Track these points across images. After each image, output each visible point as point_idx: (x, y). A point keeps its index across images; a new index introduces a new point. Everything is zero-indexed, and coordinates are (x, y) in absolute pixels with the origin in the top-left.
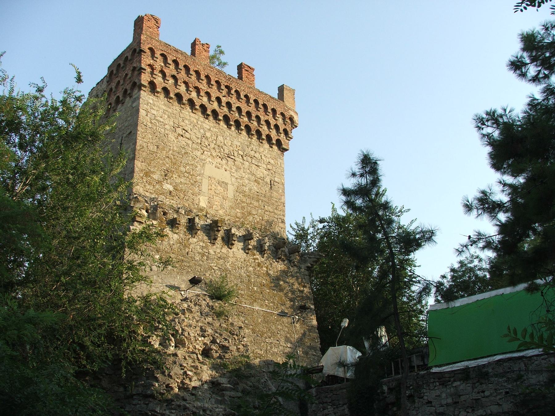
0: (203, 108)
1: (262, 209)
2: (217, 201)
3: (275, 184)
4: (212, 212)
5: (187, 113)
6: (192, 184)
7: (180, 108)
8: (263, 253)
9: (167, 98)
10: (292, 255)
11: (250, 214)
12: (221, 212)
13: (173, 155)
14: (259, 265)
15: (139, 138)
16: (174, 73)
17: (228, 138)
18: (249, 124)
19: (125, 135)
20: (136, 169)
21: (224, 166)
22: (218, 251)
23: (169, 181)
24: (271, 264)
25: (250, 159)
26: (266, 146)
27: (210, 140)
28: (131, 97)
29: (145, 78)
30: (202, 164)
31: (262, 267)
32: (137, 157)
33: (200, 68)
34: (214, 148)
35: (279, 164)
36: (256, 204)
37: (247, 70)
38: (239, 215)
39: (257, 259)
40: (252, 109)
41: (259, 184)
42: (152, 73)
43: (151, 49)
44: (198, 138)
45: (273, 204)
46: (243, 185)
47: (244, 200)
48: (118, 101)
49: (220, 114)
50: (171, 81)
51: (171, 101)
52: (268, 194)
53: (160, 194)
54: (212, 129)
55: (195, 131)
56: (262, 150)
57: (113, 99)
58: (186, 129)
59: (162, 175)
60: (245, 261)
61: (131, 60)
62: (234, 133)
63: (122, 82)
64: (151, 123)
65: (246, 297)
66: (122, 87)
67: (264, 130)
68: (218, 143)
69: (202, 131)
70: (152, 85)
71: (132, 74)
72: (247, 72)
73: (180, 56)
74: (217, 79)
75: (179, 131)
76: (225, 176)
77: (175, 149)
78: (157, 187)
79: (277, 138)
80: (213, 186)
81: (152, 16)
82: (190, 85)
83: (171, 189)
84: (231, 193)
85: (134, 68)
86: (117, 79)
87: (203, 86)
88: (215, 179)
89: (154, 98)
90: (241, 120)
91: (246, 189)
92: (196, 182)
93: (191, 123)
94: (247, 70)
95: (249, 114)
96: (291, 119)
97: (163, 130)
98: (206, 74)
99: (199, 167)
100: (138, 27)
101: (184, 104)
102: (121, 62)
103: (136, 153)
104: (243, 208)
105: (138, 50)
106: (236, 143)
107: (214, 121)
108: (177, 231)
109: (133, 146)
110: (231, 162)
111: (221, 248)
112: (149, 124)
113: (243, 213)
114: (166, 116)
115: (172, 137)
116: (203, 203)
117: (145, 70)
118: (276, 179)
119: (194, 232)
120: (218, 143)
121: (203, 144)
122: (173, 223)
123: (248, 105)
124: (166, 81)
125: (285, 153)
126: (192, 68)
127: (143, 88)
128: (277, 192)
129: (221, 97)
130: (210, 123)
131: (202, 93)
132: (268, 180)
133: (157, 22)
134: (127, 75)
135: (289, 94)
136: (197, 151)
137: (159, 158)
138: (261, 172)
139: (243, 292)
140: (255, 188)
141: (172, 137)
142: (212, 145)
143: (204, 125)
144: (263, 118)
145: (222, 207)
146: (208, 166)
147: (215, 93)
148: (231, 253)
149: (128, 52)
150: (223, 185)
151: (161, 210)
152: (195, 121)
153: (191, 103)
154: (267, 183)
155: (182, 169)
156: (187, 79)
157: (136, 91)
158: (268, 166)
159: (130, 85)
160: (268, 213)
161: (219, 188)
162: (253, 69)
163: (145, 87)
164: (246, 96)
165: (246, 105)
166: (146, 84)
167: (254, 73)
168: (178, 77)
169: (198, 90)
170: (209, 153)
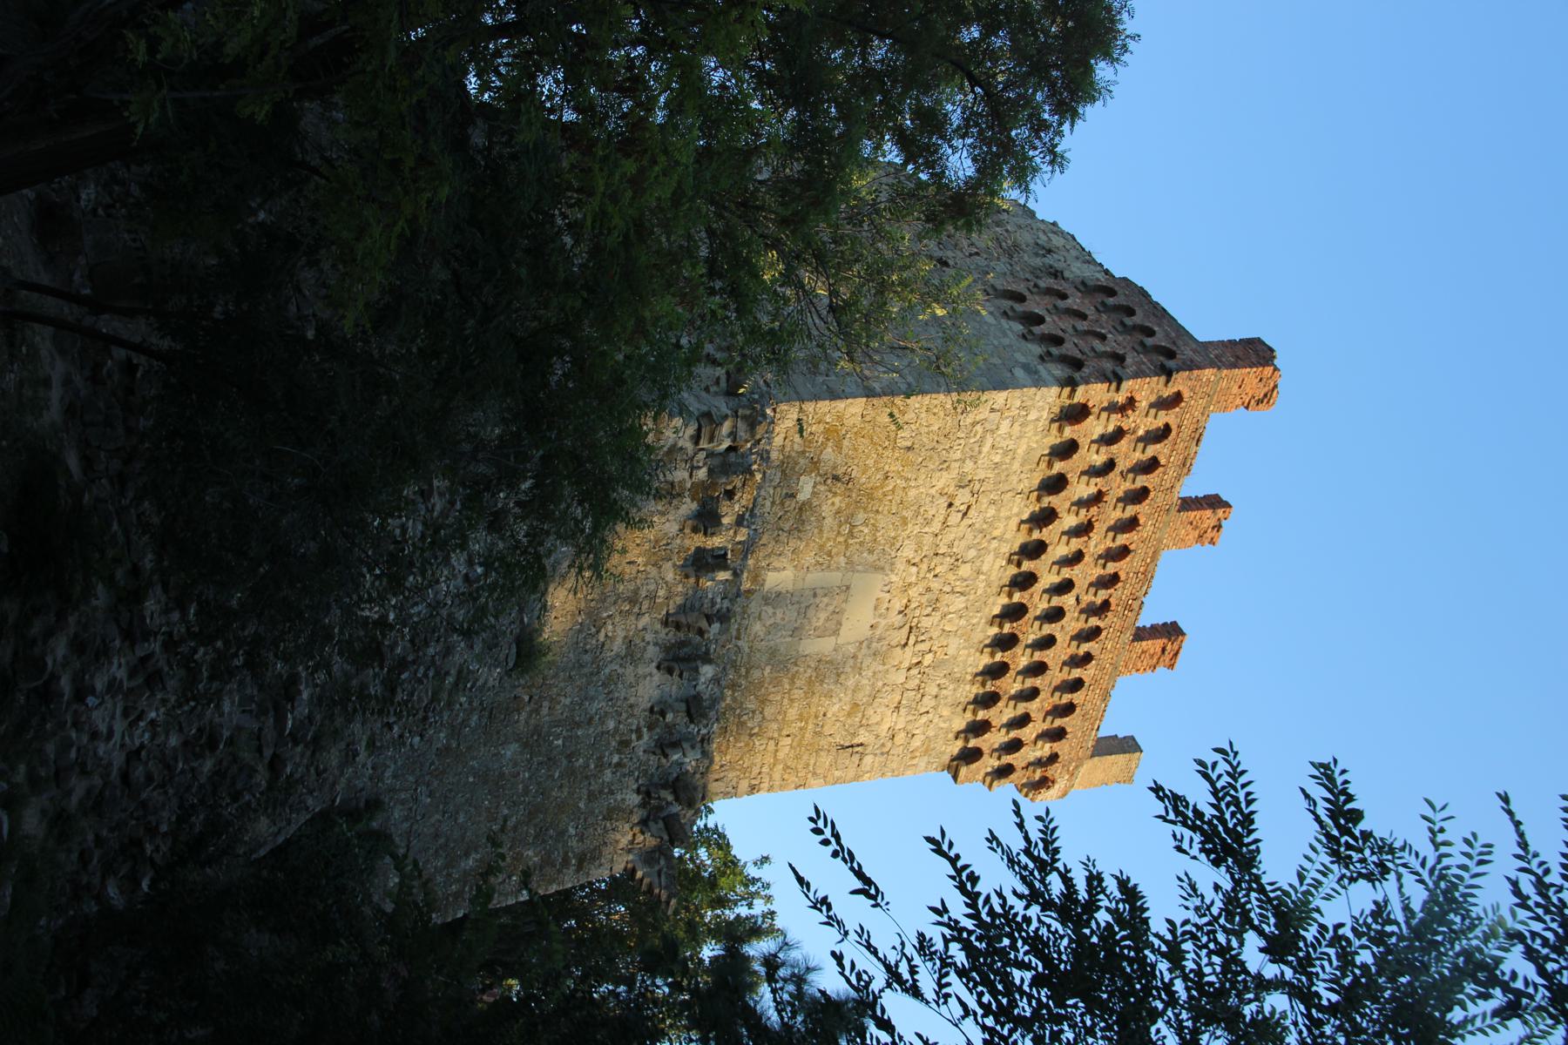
0: (1035, 550)
1: (780, 730)
3: (856, 758)
5: (1015, 510)
6: (821, 547)
7: (1026, 491)
8: (658, 751)
9: (1050, 454)
10: (661, 824)
12: (757, 628)
13: (893, 491)
15: (927, 399)
16: (1122, 465)
17: (963, 622)
18: (1012, 673)
20: (840, 405)
21: (883, 622)
23: (822, 488)
24: (631, 773)
26: (960, 723)
27: (951, 577)
28: (1041, 357)
29: (1095, 393)
31: (619, 752)
32: (875, 401)
33: (1146, 528)
34: (929, 590)
35: (915, 762)
37: (1164, 650)
39: (640, 737)
40: (1056, 675)
41: (849, 715)
42: (1113, 408)
43: (1177, 399)
44: (951, 546)
45: (798, 757)
46: (838, 675)
48: (1035, 319)
49: (1026, 594)
50: (1099, 459)
51: (1043, 465)
52: (824, 742)
53: (783, 472)
54: (982, 577)
55: (970, 536)
56: (946, 712)
57: (1036, 305)
58: (972, 513)
59: (834, 468)
60: (631, 706)
62: (980, 636)
64: (974, 424)
65: (532, 722)
66: (1070, 330)
67: (1002, 714)
68: (946, 599)
69: (972, 553)
70: (1076, 414)
71: (1100, 355)
72: (1159, 650)
73: (1171, 473)
74: (1123, 576)
75: (963, 497)
77: (912, 493)
78: (802, 461)
79: (986, 750)
80: (826, 600)
81: (1275, 386)
82: (1094, 510)
83: (802, 497)
85: (1120, 359)
86: (1090, 311)
87: (1097, 543)
88: (846, 601)
89: (1043, 423)
90: (1018, 649)
92: (829, 554)
93: (991, 525)
94: (1164, 650)
95: (1039, 669)
96: (1044, 783)
97: (958, 455)
98: (1132, 547)
100: (1240, 353)
101: (1039, 499)
102: (1138, 319)
103: (885, 399)
105: (1171, 364)
106: (954, 644)
107: (1006, 581)
108: (687, 531)
109: (904, 387)
111: (656, 644)
112: (969, 420)
114: (997, 459)
115: (944, 480)
117: (1118, 389)
118: (868, 760)
119: (691, 570)
120: (946, 599)
121: (937, 560)
122: (707, 519)
123: (1064, 663)
124: (1094, 447)
125: (947, 776)
126: (1143, 510)
127: (1067, 390)
129: (1074, 592)
130: (998, 570)
131: (1076, 543)
133: (1259, 402)
134: (1103, 338)
135: (1115, 770)
136: (914, 547)
137: (880, 456)
139: (545, 711)
141: (944, 480)
142: (935, 585)
143: (989, 558)
144: (1034, 707)
147: (1084, 574)
148: (647, 670)
149: (1167, 335)
150: (832, 625)
151: (739, 485)
152: (996, 533)
153: (1045, 517)
154: (854, 735)
155: (861, 516)
156: (1110, 499)
157: (1059, 371)
158: (903, 734)
162: (1171, 666)
163: (1071, 396)
164: (1088, 658)
165: (1064, 658)
166: (1079, 397)
167: (1161, 669)
168: (1111, 475)
169: (1084, 530)
170: (913, 579)
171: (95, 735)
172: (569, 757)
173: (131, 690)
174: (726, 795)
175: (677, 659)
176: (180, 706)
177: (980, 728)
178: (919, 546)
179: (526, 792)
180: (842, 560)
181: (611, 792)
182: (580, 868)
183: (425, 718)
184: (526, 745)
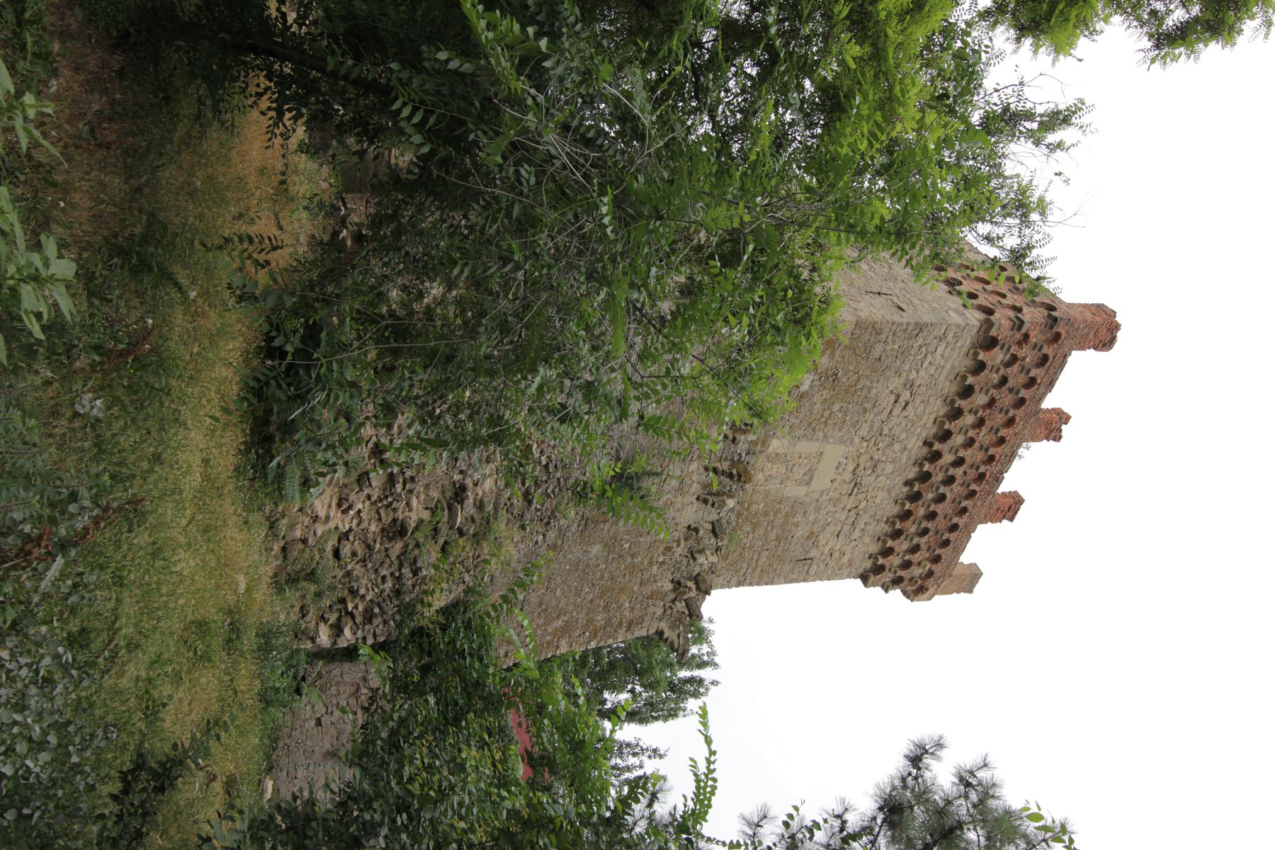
2: (778, 469)
4: (761, 461)
6: (810, 424)
10: (684, 604)
11: (755, 526)
12: (759, 477)
14: (669, 549)
19: (895, 299)
23: (817, 383)
25: (850, 521)
26: (874, 548)
27: (888, 451)
31: (664, 554)
33: (1019, 426)
36: (772, 536)
38: (754, 507)
39: (678, 546)
41: (807, 538)
55: (904, 424)
56: (867, 540)
61: (1033, 301)
63: (989, 287)
67: (902, 545)
69: (903, 436)
73: (1042, 390)
75: (906, 395)
76: (821, 482)
77: (874, 391)
84: (794, 491)
89: (965, 350)
90: (920, 503)
91: (798, 518)
92: (814, 430)
104: (766, 514)
110: (847, 488)
113: (756, 514)
115: (896, 383)
116: (776, 445)
118: (814, 568)
128: (792, 571)
130: (915, 447)
132: (814, 553)
133: (1104, 345)
134: (1004, 296)
138: (828, 541)
140: (801, 532)
141: (896, 383)
142: (876, 457)
143: (913, 440)
145: (769, 478)
146: (842, 449)
150: (806, 478)
153: (956, 414)
155: (836, 407)
159: (986, 304)
160: (755, 557)
161: (802, 472)
162: (1011, 519)
171: (315, 519)
172: (633, 556)
173: (345, 485)
174: (722, 587)
175: (710, 494)
176: (381, 500)
178: (871, 427)
179: (602, 578)
180: (821, 434)
181: (655, 581)
182: (628, 629)
183: (548, 523)
184: (606, 545)
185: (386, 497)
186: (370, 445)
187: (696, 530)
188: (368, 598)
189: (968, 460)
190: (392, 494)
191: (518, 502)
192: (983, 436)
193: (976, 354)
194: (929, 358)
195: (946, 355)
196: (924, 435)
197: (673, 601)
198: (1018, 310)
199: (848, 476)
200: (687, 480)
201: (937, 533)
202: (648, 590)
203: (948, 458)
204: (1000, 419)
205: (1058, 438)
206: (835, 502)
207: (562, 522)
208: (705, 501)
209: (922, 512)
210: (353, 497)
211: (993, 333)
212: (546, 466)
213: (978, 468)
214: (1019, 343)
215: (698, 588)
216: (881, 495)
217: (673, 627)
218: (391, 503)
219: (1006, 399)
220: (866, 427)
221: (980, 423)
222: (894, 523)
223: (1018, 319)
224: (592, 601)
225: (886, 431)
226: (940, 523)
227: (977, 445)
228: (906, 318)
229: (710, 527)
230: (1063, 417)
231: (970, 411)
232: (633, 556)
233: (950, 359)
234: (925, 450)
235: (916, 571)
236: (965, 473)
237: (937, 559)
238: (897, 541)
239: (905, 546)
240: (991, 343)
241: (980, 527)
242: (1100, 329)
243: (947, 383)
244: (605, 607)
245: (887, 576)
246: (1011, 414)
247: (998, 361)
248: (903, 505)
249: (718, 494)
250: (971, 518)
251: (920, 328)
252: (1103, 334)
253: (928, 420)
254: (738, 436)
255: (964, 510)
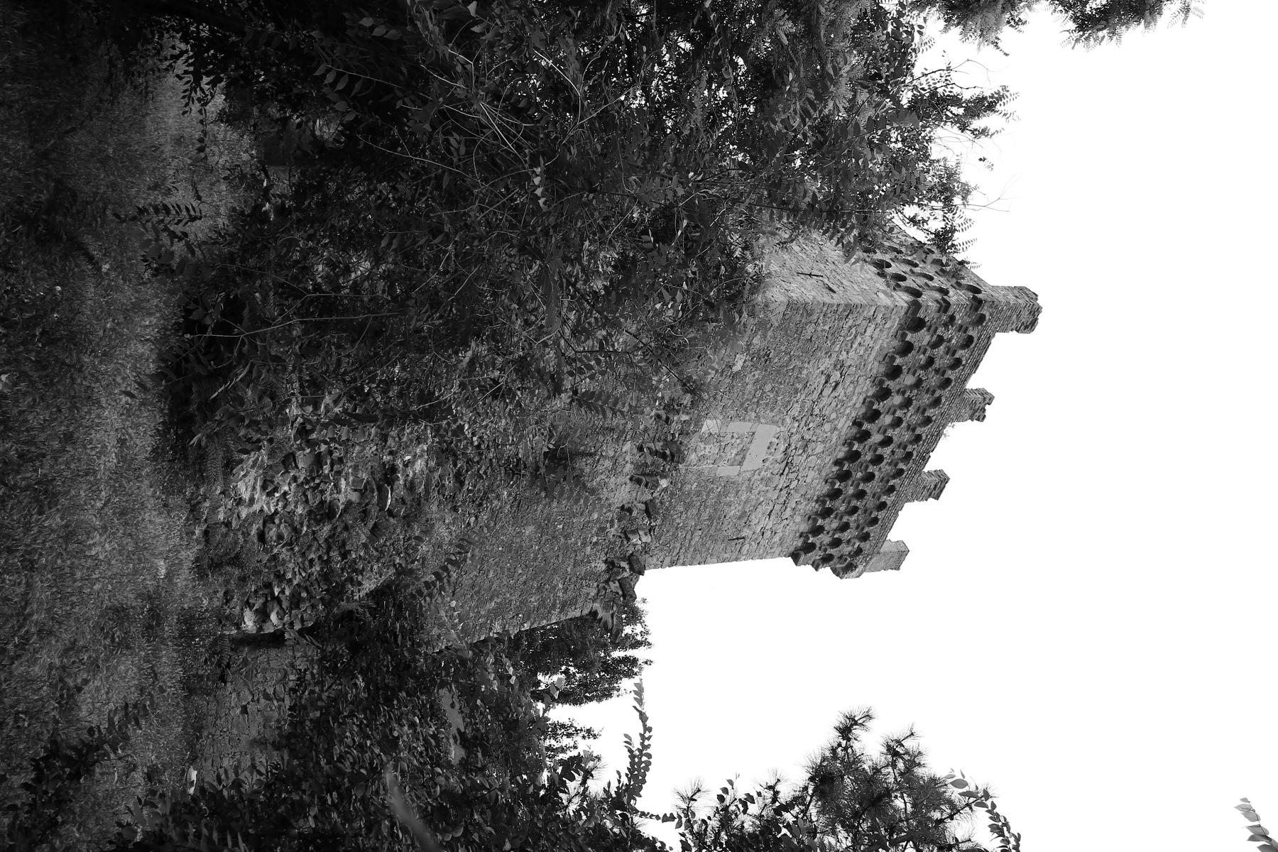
2: (710, 449)
4: (694, 441)
6: (742, 405)
11: (688, 507)
12: (693, 457)
14: (602, 529)
19: (826, 281)
22: (627, 458)
25: (782, 500)
26: (804, 527)
27: (818, 431)
30: (776, 419)
36: (705, 516)
38: (687, 488)
39: (612, 526)
41: (740, 518)
47: (712, 495)
55: (834, 404)
58: (840, 388)
67: (831, 524)
69: (834, 416)
73: (967, 371)
75: (836, 376)
76: (753, 462)
77: (805, 372)
83: (735, 369)
84: (725, 471)
91: (731, 498)
99: (772, 414)
110: (778, 468)
115: (826, 363)
116: (709, 425)
130: (844, 426)
132: (746, 532)
133: (1026, 327)
134: (931, 279)
138: (759, 520)
140: (733, 512)
141: (826, 363)
142: (807, 437)
146: (775, 429)
153: (884, 394)
155: (768, 387)
159: (915, 286)
160: (689, 537)
161: (735, 452)
162: (937, 498)
171: (239, 501)
172: (566, 537)
173: (270, 467)
174: (656, 567)
175: (644, 474)
176: (307, 482)
177: (817, 531)
178: (802, 407)
179: (535, 559)
180: (753, 414)
182: (562, 610)
183: (481, 504)
184: (540, 526)
185: (313, 479)
186: (296, 425)
187: (630, 510)
188: (295, 582)
189: (895, 439)
190: (319, 476)
191: (449, 483)
192: (911, 416)
193: (904, 335)
194: (859, 339)
195: (875, 336)
196: (854, 415)
197: (607, 582)
198: (944, 292)
199: (779, 456)
200: (620, 460)
201: (866, 511)
202: (582, 570)
203: (877, 438)
204: (926, 399)
205: (981, 418)
206: (767, 481)
207: (496, 502)
208: (639, 482)
209: (851, 491)
210: (278, 478)
211: (921, 315)
212: (478, 447)
213: (905, 448)
214: (946, 325)
215: (632, 569)
216: (812, 474)
217: (607, 607)
218: (318, 485)
219: (933, 380)
220: (797, 407)
221: (907, 403)
222: (824, 502)
223: (945, 301)
224: (525, 583)
225: (817, 411)
226: (870, 502)
227: (904, 424)
228: (836, 299)
229: (643, 507)
230: (987, 398)
231: (898, 392)
232: (566, 537)
233: (877, 340)
234: (855, 430)
235: (846, 549)
236: (893, 452)
237: (865, 537)
238: (827, 520)
239: (835, 525)
240: (917, 324)
241: (907, 505)
242: (1023, 313)
243: (876, 364)
244: (538, 588)
245: (817, 555)
246: (937, 395)
247: (925, 343)
248: (833, 484)
249: (651, 474)
250: (898, 496)
251: (850, 309)
252: (1025, 317)
253: (857, 400)
254: (671, 416)
255: (892, 489)
